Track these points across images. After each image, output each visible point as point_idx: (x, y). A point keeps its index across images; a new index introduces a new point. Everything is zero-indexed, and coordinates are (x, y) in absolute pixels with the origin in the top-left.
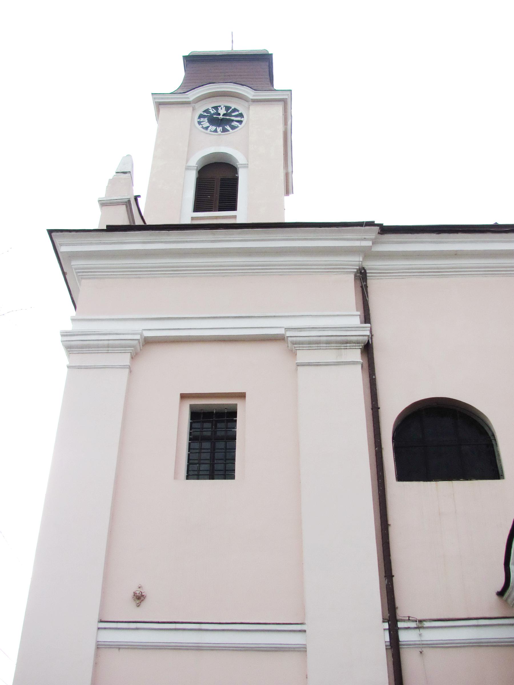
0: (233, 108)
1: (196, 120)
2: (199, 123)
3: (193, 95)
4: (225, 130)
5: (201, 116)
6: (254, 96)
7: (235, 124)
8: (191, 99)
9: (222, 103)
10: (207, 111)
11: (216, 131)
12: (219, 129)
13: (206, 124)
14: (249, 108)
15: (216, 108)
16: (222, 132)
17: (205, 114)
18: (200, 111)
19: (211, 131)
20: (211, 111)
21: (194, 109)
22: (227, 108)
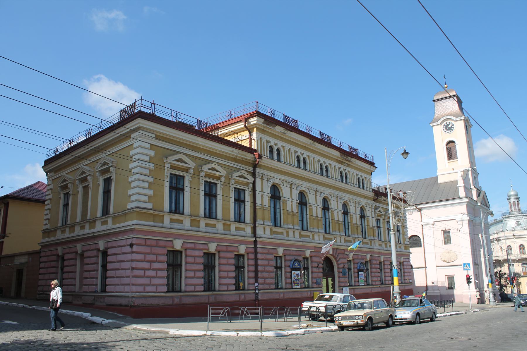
1: (442, 129)
2: (444, 129)
4: (450, 132)
5: (443, 127)
7: (453, 126)
8: (439, 123)
10: (444, 125)
11: (448, 132)
12: (449, 131)
13: (445, 130)
15: (446, 123)
17: (444, 126)
22: (449, 122)
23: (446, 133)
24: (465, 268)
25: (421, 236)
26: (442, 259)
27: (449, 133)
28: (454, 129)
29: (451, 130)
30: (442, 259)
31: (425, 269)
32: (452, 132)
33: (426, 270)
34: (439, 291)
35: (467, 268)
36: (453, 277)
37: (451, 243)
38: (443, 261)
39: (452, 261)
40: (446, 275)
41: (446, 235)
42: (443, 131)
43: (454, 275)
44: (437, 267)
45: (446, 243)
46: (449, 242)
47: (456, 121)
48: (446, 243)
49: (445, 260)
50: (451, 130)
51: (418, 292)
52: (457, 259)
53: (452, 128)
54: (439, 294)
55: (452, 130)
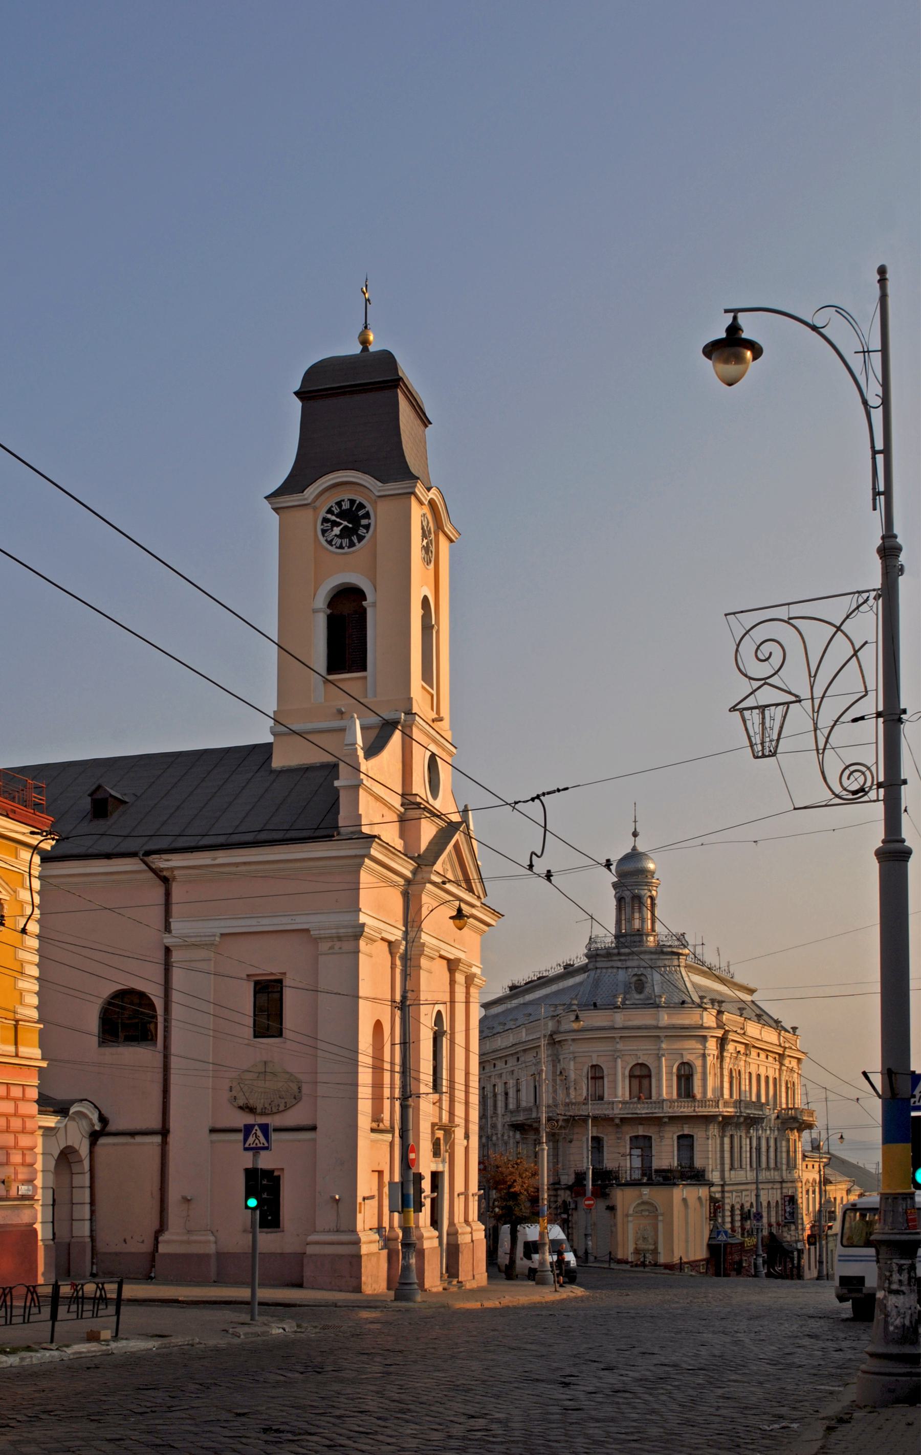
0: (357, 502)
1: (319, 527)
3: (311, 492)
4: (352, 545)
6: (379, 491)
8: (309, 501)
9: (346, 495)
10: (330, 511)
11: (341, 547)
12: (346, 542)
14: (376, 502)
15: (339, 504)
16: (349, 547)
18: (322, 513)
19: (337, 548)
20: (334, 509)
21: (315, 509)
22: (352, 502)
23: (333, 549)
24: (251, 1139)
25: (155, 993)
26: (235, 1098)
27: (346, 550)
28: (368, 536)
29: (355, 539)
31: (158, 1139)
32: (358, 546)
33: (164, 1144)
35: (257, 1141)
37: (280, 1034)
38: (241, 1108)
39: (275, 1110)
42: (322, 539)
44: (213, 1131)
45: (260, 1032)
47: (380, 497)
48: (260, 1032)
50: (355, 539)
51: (125, 1241)
53: (362, 531)
55: (361, 538)
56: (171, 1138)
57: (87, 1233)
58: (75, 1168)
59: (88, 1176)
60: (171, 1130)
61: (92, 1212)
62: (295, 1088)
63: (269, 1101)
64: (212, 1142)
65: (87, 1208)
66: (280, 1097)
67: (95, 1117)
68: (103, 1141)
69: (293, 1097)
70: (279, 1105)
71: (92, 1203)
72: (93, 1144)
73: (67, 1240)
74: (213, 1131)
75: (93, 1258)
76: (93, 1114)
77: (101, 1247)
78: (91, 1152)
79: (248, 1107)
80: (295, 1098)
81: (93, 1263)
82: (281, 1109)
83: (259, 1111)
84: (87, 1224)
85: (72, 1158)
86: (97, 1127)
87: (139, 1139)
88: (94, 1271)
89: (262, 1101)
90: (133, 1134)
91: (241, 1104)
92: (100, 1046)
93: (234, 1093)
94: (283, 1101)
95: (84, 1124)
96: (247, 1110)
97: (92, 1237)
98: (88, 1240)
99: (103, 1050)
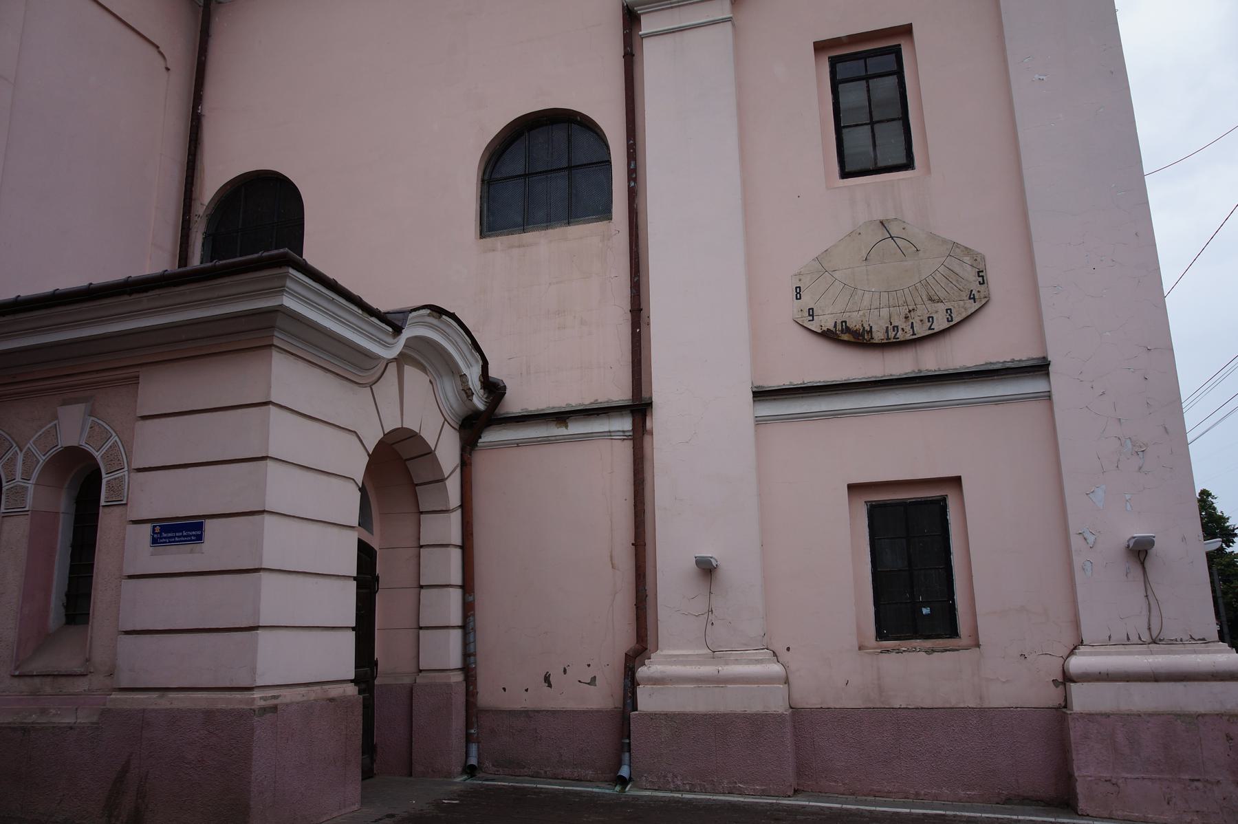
26: (811, 312)
30: (811, 312)
31: (624, 424)
34: (776, 669)
36: (940, 506)
38: (828, 335)
39: (922, 331)
40: (852, 488)
41: (854, 95)
43: (956, 481)
44: (761, 395)
46: (889, 135)
49: (854, 323)
51: (547, 679)
52: (979, 301)
54: (776, 703)
56: (659, 420)
57: (454, 658)
58: (427, 500)
59: (456, 518)
60: (656, 399)
61: (468, 608)
62: (970, 275)
63: (904, 310)
64: (759, 421)
65: (455, 598)
66: (931, 299)
67: (473, 375)
68: (491, 436)
69: (965, 295)
70: (930, 319)
71: (467, 586)
72: (469, 445)
73: (407, 681)
74: (761, 395)
75: (468, 725)
76: (469, 366)
77: (488, 696)
78: (465, 465)
79: (847, 330)
80: (972, 298)
81: (469, 739)
82: (937, 327)
83: (878, 336)
84: (455, 639)
85: (419, 471)
86: (479, 403)
87: (576, 428)
88: (473, 761)
89: (884, 312)
90: (561, 417)
91: (829, 325)
92: (482, 235)
93: (807, 300)
94: (941, 307)
95: (449, 388)
96: (845, 337)
97: (468, 670)
98: (458, 678)
99: (489, 241)
